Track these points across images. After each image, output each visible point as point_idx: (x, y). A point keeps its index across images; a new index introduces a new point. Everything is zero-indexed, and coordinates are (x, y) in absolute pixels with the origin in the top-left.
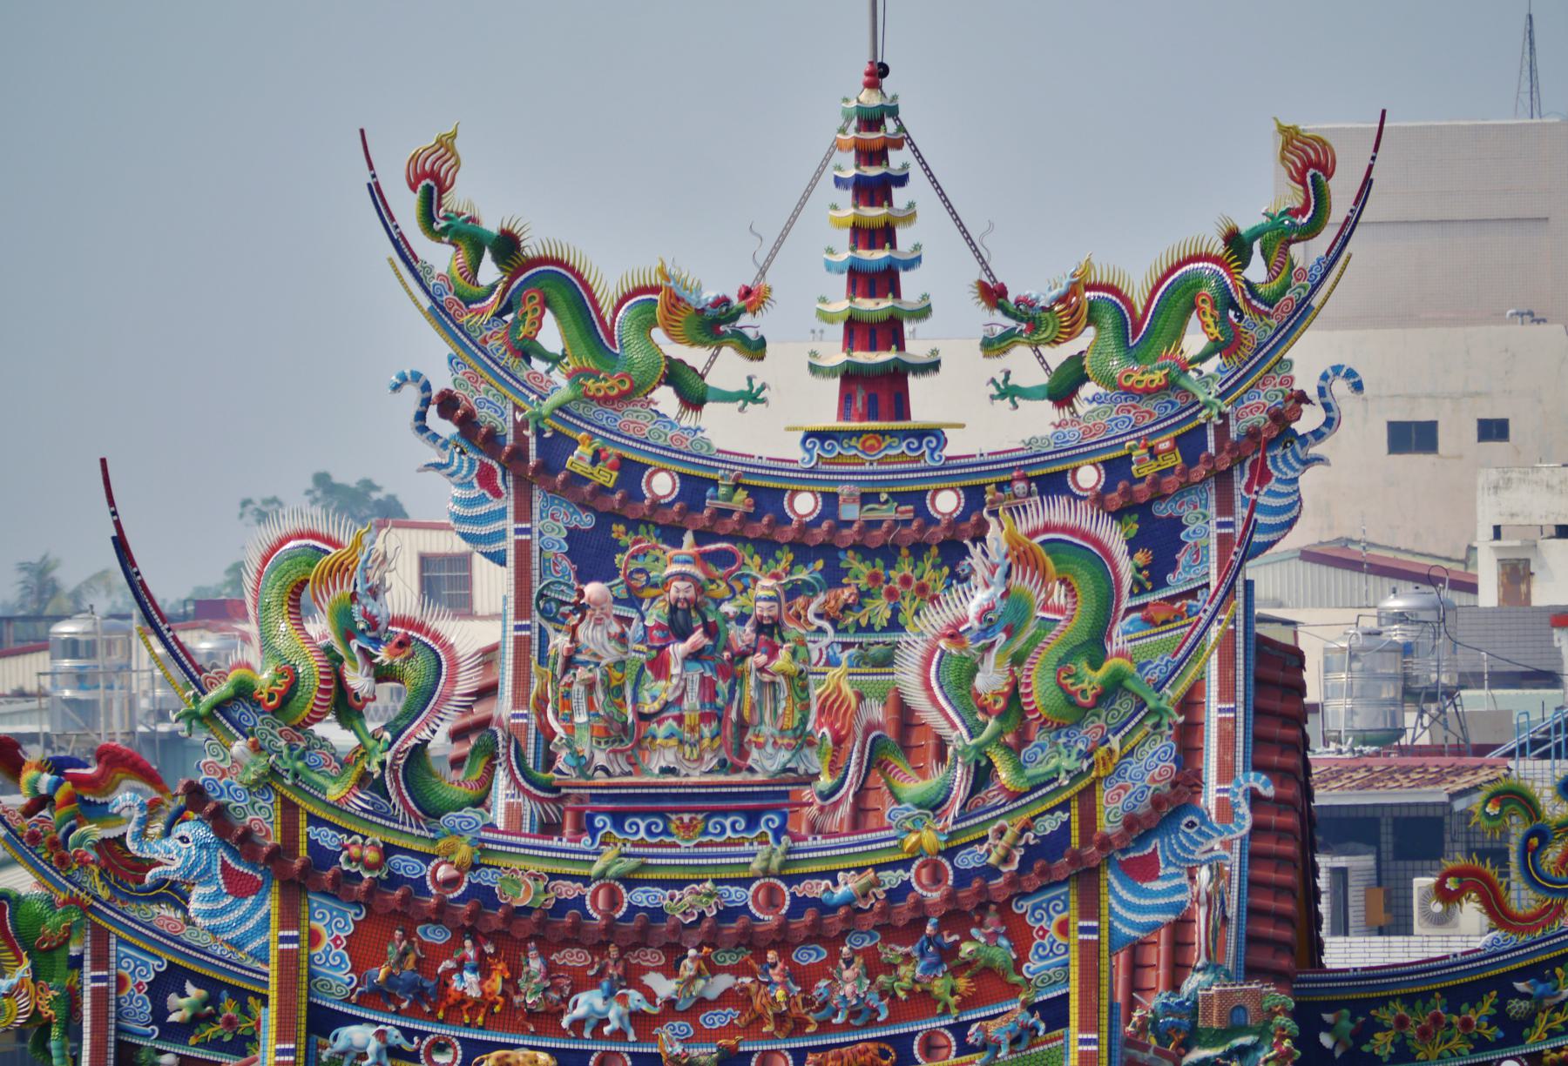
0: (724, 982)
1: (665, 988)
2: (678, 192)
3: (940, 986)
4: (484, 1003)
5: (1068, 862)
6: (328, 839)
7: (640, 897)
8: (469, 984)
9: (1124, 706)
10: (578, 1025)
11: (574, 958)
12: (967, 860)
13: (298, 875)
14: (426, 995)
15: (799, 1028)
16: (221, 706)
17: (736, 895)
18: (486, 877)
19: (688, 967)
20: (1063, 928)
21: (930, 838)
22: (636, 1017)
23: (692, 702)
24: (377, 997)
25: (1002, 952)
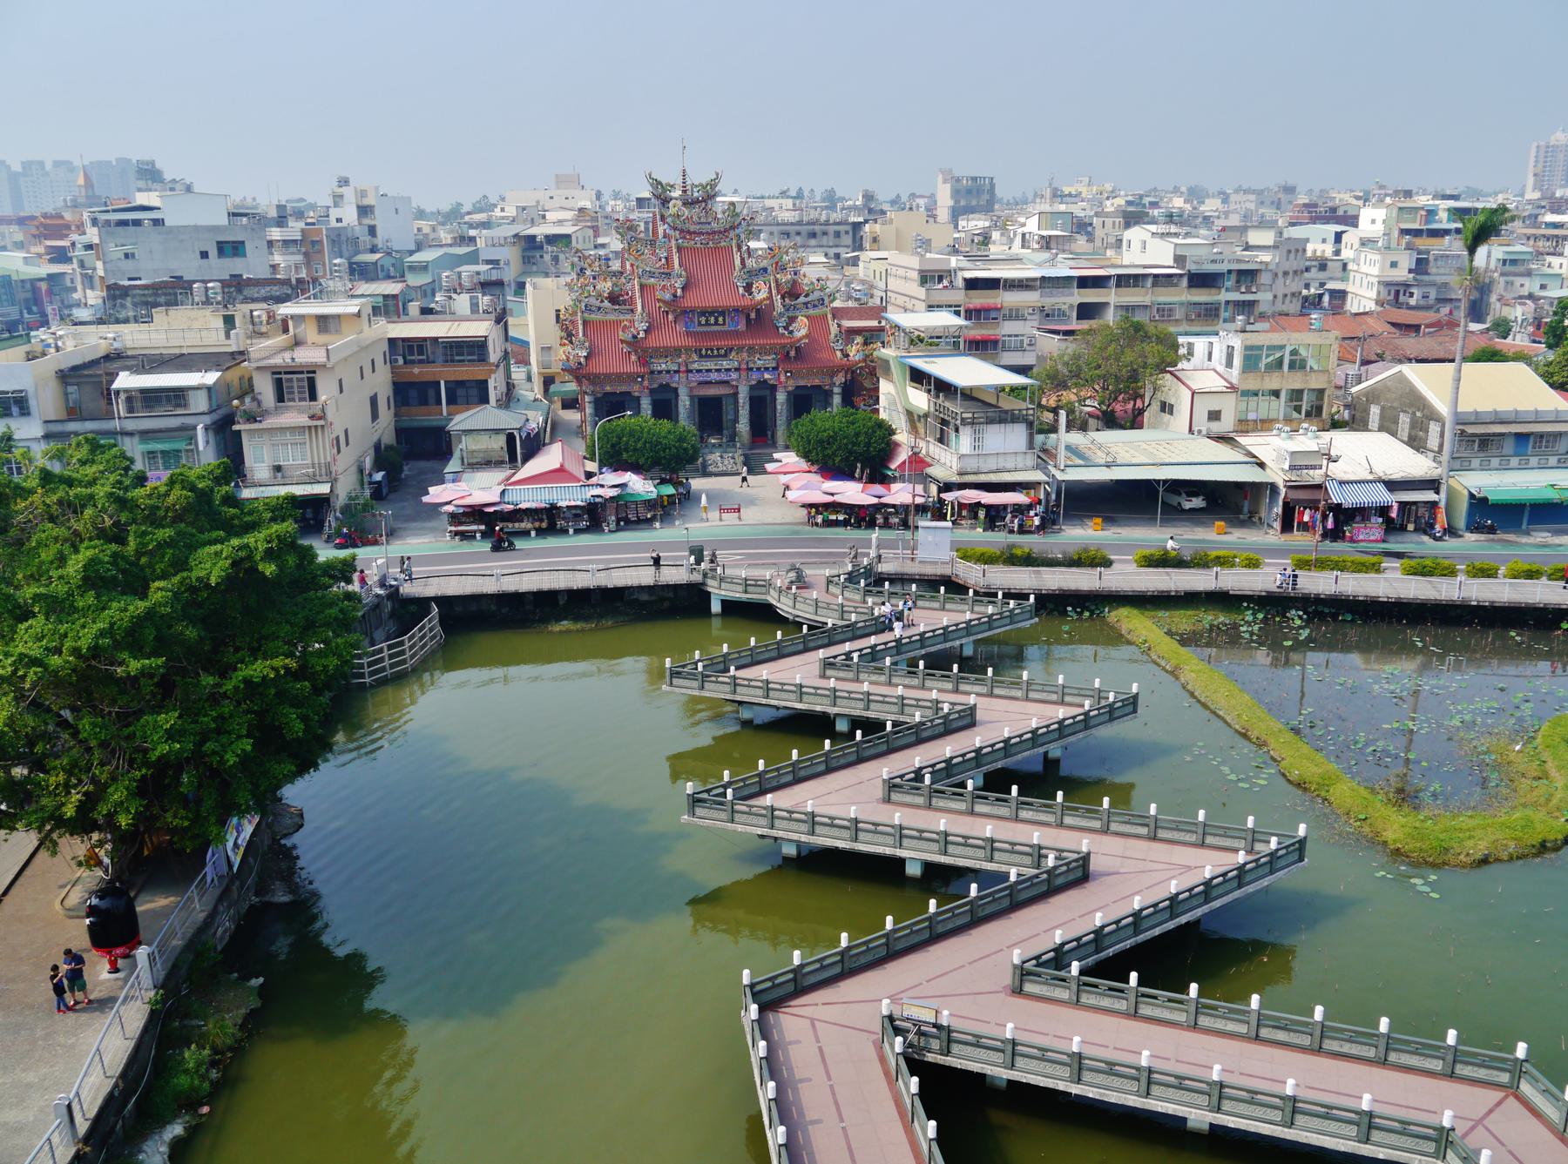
2: (670, 176)
5: (733, 228)
13: (675, 229)
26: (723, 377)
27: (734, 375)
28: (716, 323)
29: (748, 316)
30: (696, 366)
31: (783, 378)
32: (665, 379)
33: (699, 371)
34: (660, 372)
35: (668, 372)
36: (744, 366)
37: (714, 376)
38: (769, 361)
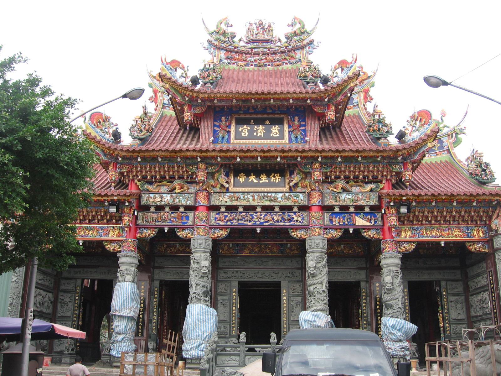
0: (264, 58)
1: (257, 58)
3: (287, 57)
4: (238, 59)
6: (223, 45)
7: (256, 50)
8: (237, 57)
9: (306, 34)
10: (249, 61)
11: (248, 55)
12: (290, 47)
14: (232, 59)
15: (272, 61)
16: (213, 33)
17: (265, 50)
18: (239, 48)
19: (260, 55)
20: (300, 53)
21: (287, 44)
22: (255, 60)
23: (261, 32)
24: (227, 58)
25: (294, 55)
26: (276, 220)
27: (297, 218)
28: (267, 136)
29: (321, 117)
30: (225, 200)
31: (392, 220)
32: (168, 220)
33: (231, 209)
34: (160, 208)
35: (175, 208)
36: (315, 200)
37: (259, 220)
38: (364, 194)
